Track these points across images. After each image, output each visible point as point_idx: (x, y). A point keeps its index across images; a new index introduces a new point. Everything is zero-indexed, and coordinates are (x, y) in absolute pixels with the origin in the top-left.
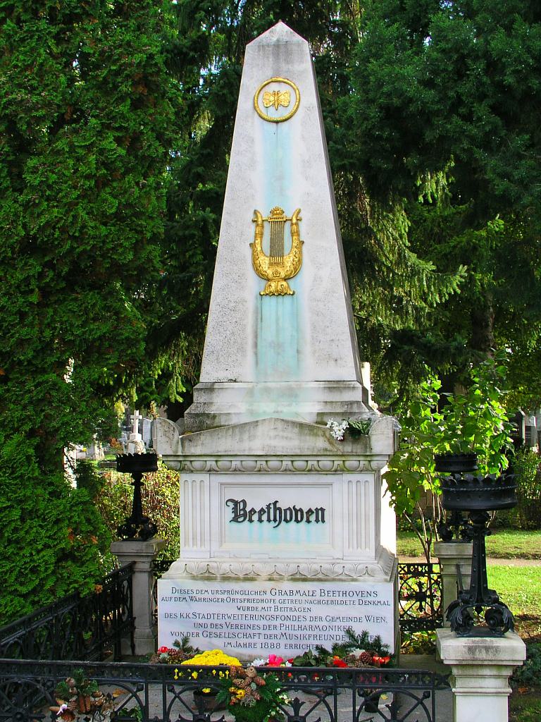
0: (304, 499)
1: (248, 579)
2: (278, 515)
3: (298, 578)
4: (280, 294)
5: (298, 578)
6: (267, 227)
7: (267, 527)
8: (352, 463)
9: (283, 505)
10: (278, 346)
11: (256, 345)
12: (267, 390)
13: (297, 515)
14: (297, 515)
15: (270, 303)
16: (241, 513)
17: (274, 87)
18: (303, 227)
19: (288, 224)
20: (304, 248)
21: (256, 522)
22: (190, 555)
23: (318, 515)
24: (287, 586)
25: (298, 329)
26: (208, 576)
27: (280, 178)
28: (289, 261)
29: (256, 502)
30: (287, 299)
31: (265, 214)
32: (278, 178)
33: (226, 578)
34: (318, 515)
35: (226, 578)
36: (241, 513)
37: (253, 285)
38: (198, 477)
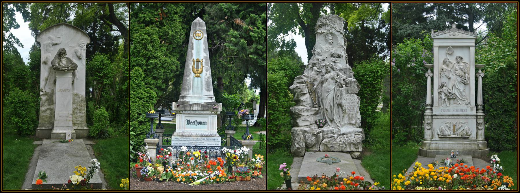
0: (202, 120)
1: (191, 136)
2: (197, 123)
3: (202, 136)
4: (199, 77)
5: (202, 136)
6: (196, 63)
7: (194, 125)
8: (213, 113)
9: (198, 121)
10: (197, 88)
13: (200, 123)
14: (200, 123)
15: (196, 78)
16: (189, 122)
17: (198, 32)
22: (178, 131)
23: (205, 123)
24: (199, 138)
25: (202, 85)
26: (183, 136)
27: (199, 52)
28: (200, 70)
29: (192, 120)
30: (200, 78)
31: (195, 60)
32: (198, 52)
33: (186, 136)
34: (205, 123)
35: (186, 136)
36: (189, 122)
37: (193, 74)
38: (180, 115)
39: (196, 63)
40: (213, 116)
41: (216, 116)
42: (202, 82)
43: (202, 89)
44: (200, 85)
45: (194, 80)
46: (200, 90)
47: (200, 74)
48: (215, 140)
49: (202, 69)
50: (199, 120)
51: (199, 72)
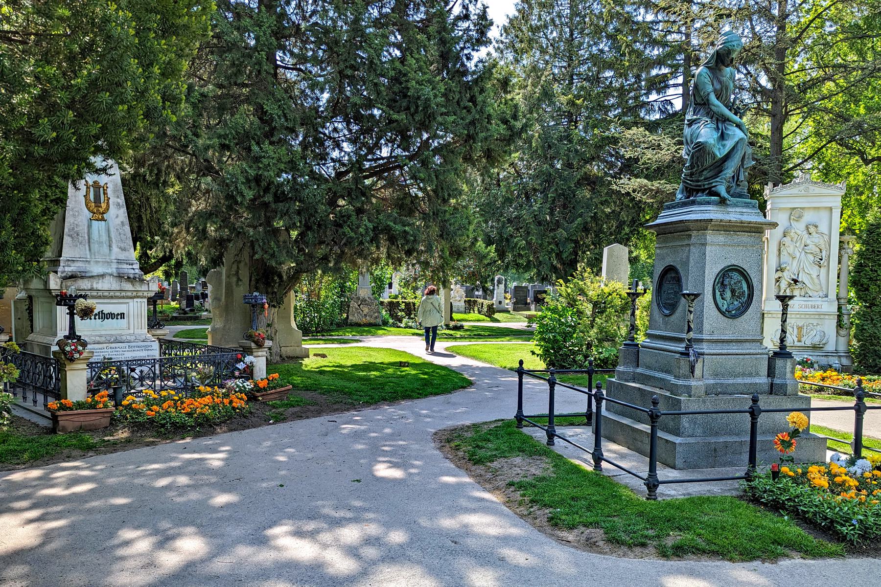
4: (103, 219)
6: (92, 189)
7: (99, 321)
9: (105, 312)
10: (100, 243)
11: (89, 242)
12: (97, 262)
13: (111, 316)
14: (111, 316)
18: (109, 191)
19: (101, 189)
20: (110, 201)
21: (93, 320)
23: (122, 316)
28: (104, 205)
30: (103, 222)
34: (122, 316)
39: (92, 189)
40: (139, 300)
41: (146, 300)
42: (109, 231)
43: (110, 246)
44: (104, 238)
45: (90, 227)
46: (105, 249)
47: (103, 213)
48: (147, 348)
49: (108, 204)
50: (107, 309)
51: (101, 210)
